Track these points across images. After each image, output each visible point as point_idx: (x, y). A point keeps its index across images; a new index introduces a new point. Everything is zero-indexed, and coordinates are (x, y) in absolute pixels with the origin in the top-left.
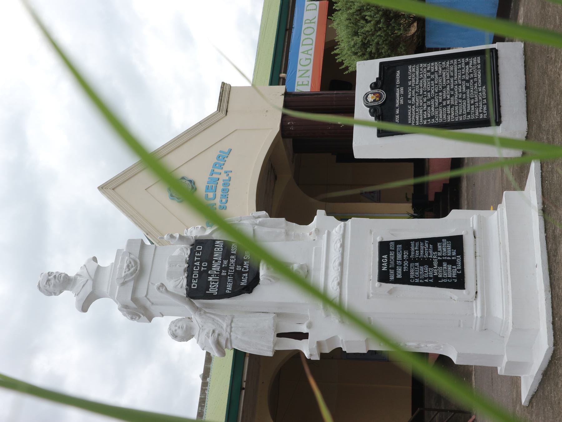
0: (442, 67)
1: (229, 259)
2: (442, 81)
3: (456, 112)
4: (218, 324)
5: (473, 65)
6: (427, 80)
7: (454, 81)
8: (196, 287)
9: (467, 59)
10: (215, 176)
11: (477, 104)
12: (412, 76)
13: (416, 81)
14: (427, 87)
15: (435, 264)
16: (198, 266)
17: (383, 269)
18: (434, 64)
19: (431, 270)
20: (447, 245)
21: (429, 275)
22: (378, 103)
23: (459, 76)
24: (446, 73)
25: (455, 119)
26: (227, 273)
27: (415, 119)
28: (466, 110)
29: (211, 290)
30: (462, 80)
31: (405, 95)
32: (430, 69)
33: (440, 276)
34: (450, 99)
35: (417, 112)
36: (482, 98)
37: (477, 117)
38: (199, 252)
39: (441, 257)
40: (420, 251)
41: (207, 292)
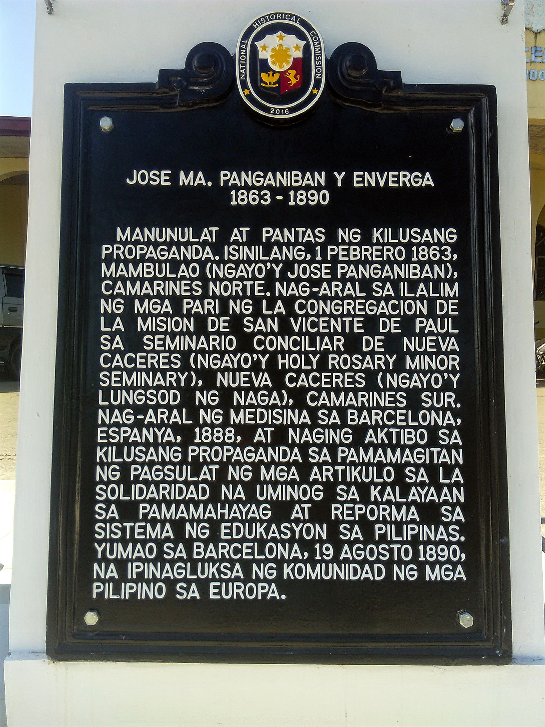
0: (423, 390)
2: (338, 391)
5: (415, 541)
7: (333, 448)
9: (459, 515)
11: (181, 551)
12: (388, 244)
13: (356, 263)
14: (317, 316)
18: (447, 354)
23: (355, 473)
24: (384, 409)
25: (109, 444)
28: (152, 501)
32: (422, 333)
34: (225, 424)
35: (175, 268)
36: (207, 581)
37: (100, 550)
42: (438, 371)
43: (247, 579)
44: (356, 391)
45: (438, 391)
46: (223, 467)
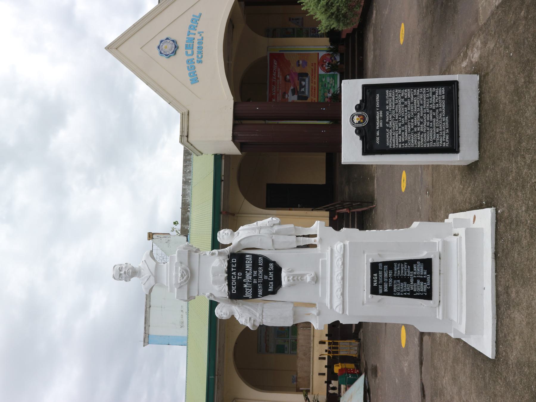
1: (257, 270)
2: (414, 108)
3: (425, 139)
4: (253, 313)
5: (438, 96)
6: (401, 106)
7: (423, 109)
8: (235, 292)
9: (434, 89)
10: (191, 36)
11: (441, 132)
12: (389, 101)
13: (392, 106)
14: (401, 112)
15: (412, 281)
16: (235, 275)
17: (374, 285)
18: (407, 91)
19: (408, 286)
20: (420, 266)
21: (407, 289)
22: (362, 125)
24: (417, 101)
26: (257, 281)
27: (392, 142)
28: (433, 138)
29: (247, 294)
30: (430, 109)
31: (384, 118)
32: (404, 95)
33: (415, 290)
34: (420, 126)
35: (394, 136)
36: (446, 128)
38: (234, 264)
39: (416, 275)
40: (401, 271)
41: (244, 296)
42: (410, 92)
43: (445, 122)
44: (414, 105)
45: (414, 92)
46: (427, 126)
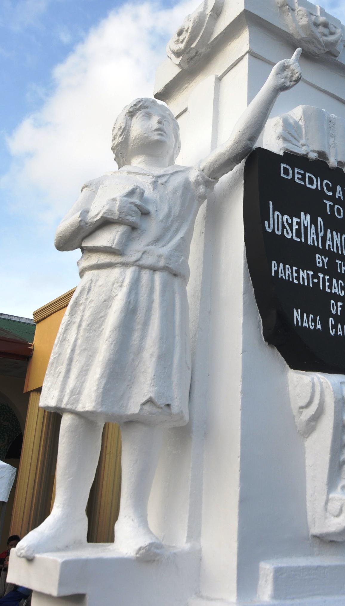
26: (322, 270)
